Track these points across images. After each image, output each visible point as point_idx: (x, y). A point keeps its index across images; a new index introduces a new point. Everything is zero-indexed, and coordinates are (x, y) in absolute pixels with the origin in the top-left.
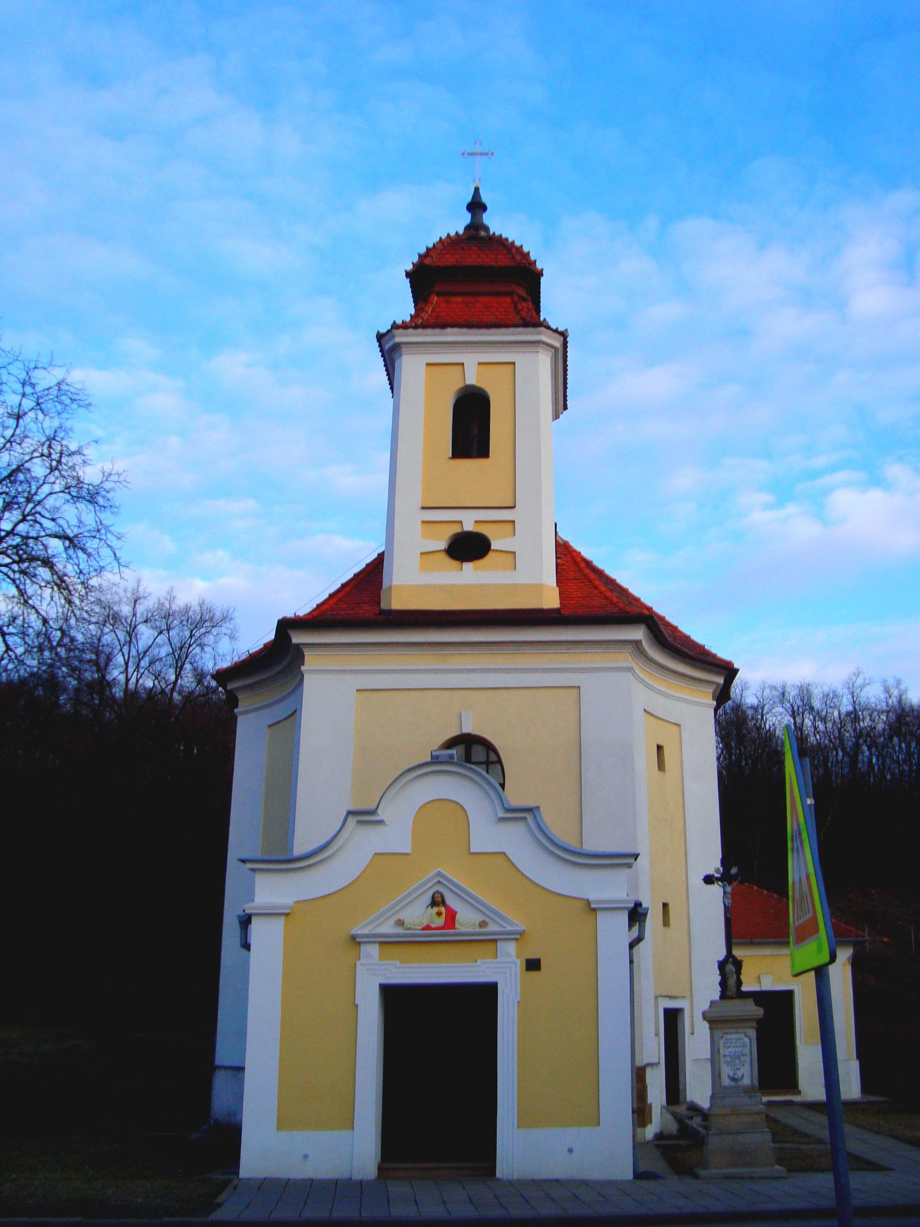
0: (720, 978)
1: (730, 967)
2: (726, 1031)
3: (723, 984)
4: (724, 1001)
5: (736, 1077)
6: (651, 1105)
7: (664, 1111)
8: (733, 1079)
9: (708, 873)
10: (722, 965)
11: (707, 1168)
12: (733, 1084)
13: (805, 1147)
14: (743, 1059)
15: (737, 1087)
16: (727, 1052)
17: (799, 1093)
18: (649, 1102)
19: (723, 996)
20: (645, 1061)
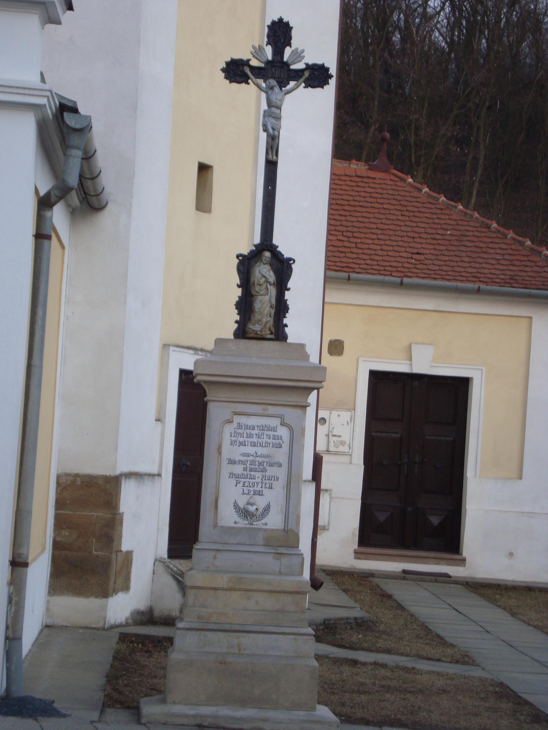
0: (239, 292)
1: (264, 272)
2: (241, 408)
3: (245, 306)
4: (244, 343)
5: (252, 509)
6: (129, 554)
7: (160, 568)
8: (245, 513)
9: (237, 56)
10: (246, 264)
11: (164, 701)
12: (243, 523)
13: (423, 666)
14: (271, 471)
15: (252, 532)
16: (237, 453)
17: (463, 562)
18: (125, 547)
19: (242, 333)
20: (122, 467)
